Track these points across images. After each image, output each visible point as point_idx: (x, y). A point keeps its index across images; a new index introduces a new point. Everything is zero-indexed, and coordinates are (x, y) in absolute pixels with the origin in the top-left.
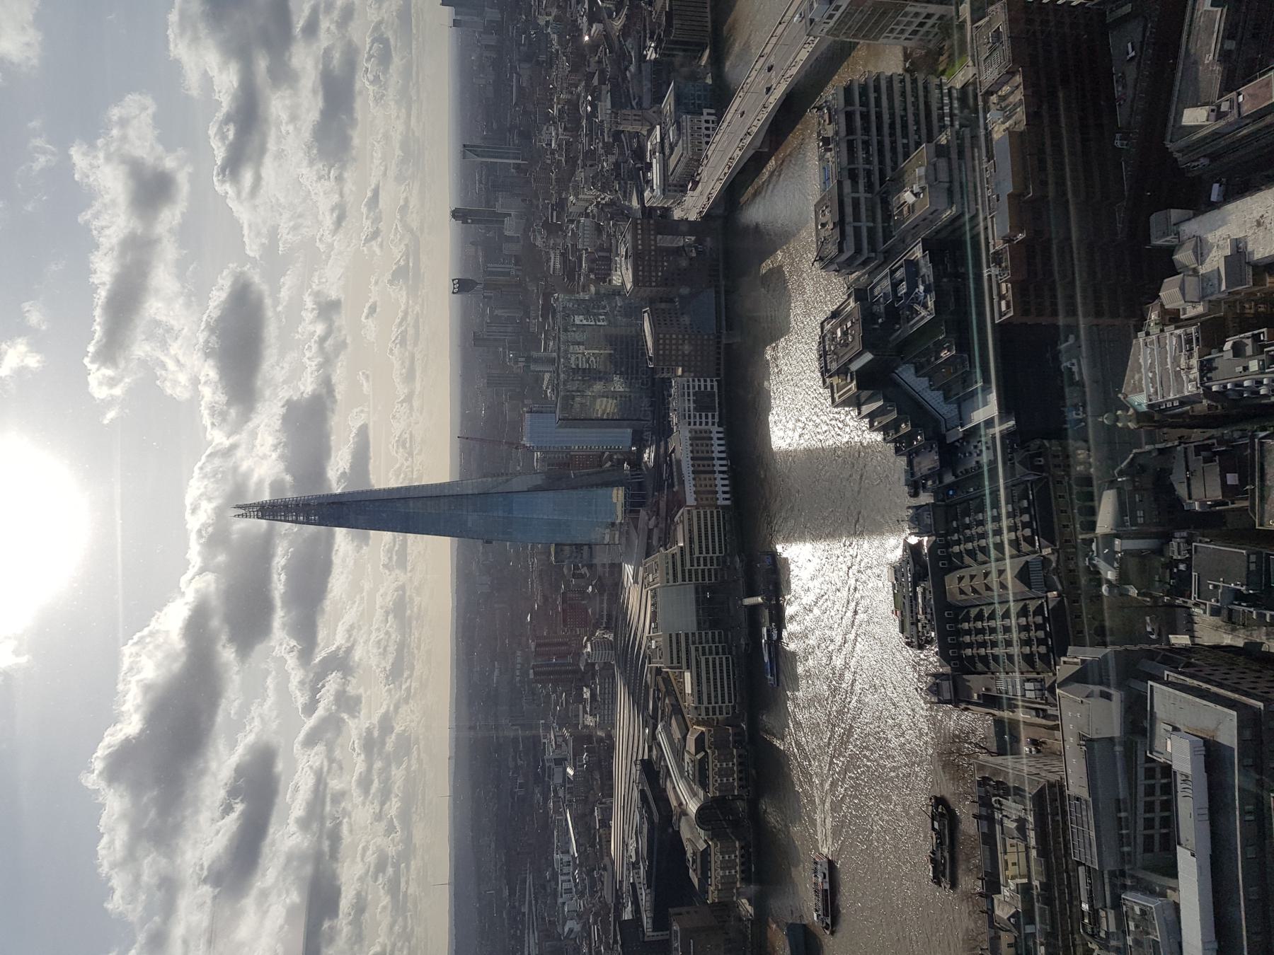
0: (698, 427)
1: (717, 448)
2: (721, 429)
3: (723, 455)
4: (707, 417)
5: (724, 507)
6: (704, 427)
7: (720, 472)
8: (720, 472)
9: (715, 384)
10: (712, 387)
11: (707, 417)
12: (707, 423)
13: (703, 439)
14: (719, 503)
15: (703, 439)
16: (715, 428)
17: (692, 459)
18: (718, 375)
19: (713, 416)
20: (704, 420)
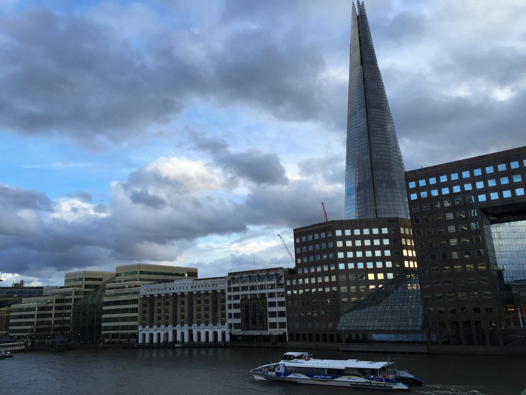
0: (228, 302)
1: (205, 331)
2: (228, 338)
3: (195, 339)
4: (236, 316)
5: (136, 336)
6: (228, 311)
7: (175, 332)
8: (175, 332)
9: (277, 331)
10: (273, 325)
11: (236, 316)
12: (230, 316)
13: (215, 309)
14: (140, 328)
15: (215, 309)
16: (226, 329)
17: (190, 293)
18: (291, 335)
19: (237, 326)
20: (234, 311)
